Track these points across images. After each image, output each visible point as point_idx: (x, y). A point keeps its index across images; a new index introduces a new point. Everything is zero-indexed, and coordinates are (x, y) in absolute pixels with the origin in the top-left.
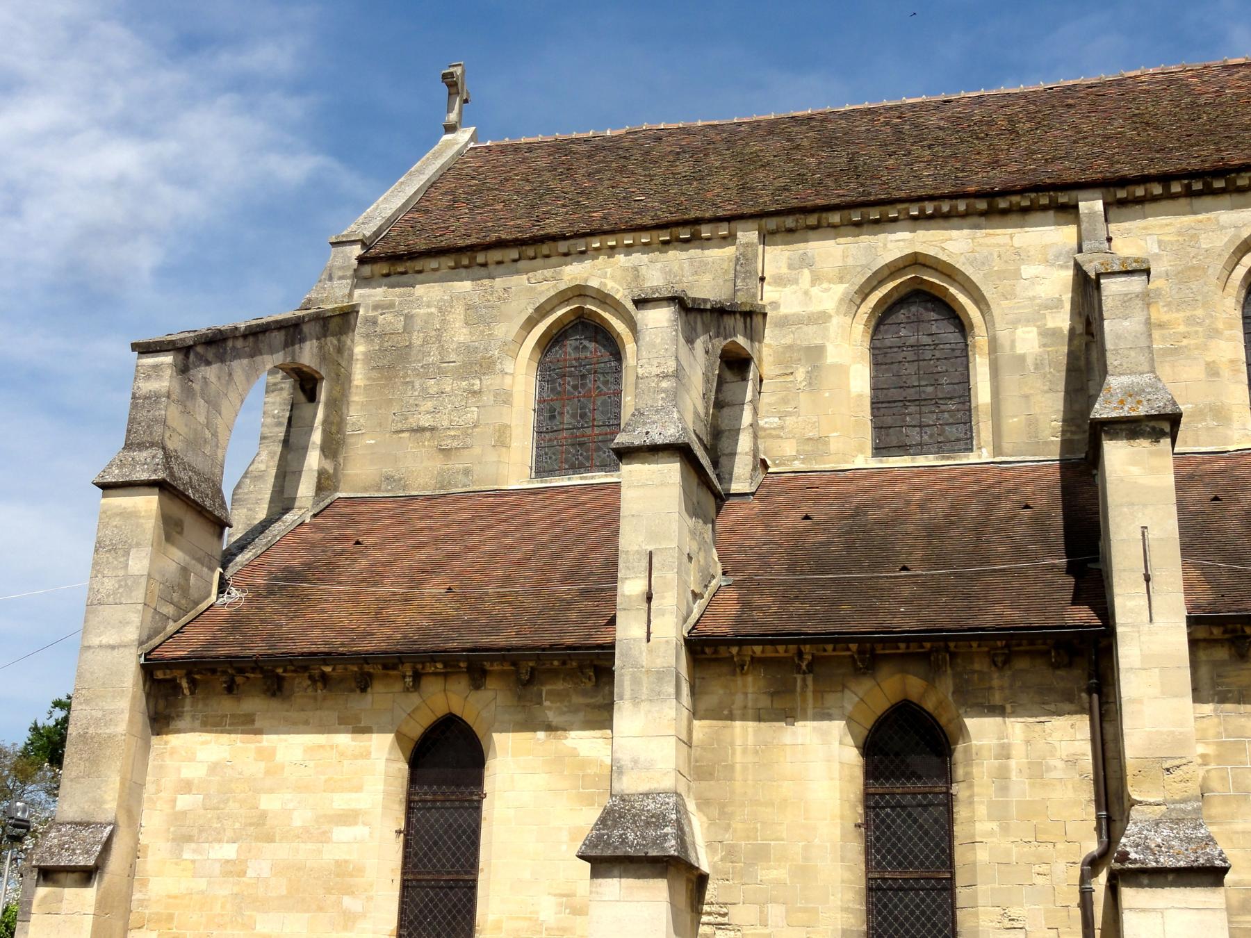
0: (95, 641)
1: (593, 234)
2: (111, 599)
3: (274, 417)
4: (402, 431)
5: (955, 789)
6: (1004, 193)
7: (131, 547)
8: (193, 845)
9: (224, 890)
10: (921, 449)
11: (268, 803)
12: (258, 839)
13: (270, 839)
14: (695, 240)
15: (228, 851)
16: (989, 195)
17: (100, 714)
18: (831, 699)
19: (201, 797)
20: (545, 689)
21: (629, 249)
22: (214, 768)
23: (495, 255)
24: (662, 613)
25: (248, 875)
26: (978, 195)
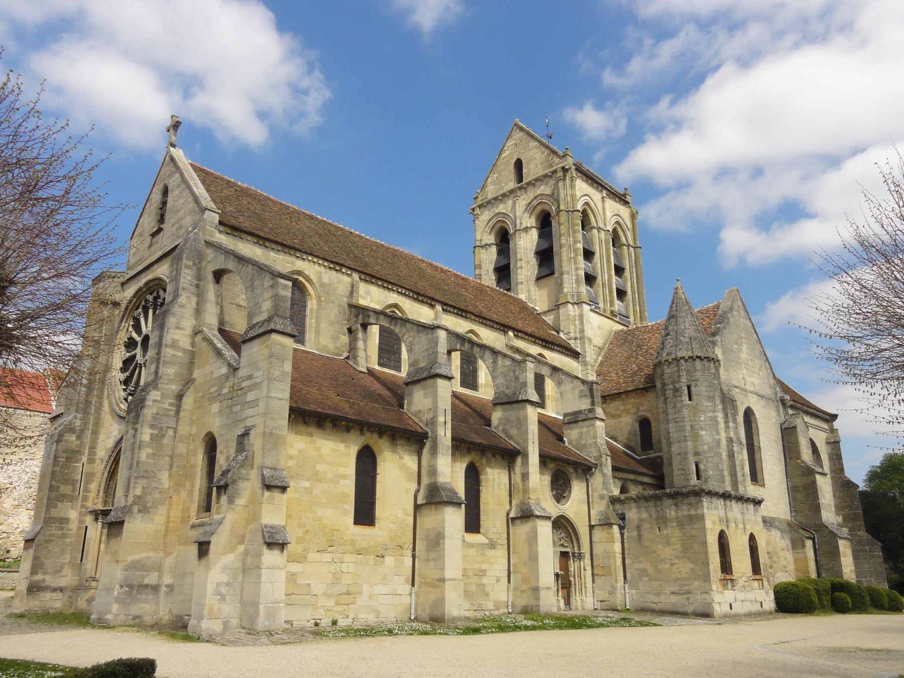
0: (273, 395)
1: (311, 254)
2: (278, 379)
3: (189, 280)
4: (233, 304)
5: (481, 488)
6: (422, 295)
7: (284, 359)
8: (294, 480)
10: (389, 368)
11: (319, 468)
13: (320, 481)
15: (307, 484)
16: (418, 294)
17: (277, 425)
18: (463, 459)
19: (296, 462)
20: (399, 442)
22: (300, 451)
23: (274, 246)
24: (448, 429)
25: (314, 493)
26: (416, 293)
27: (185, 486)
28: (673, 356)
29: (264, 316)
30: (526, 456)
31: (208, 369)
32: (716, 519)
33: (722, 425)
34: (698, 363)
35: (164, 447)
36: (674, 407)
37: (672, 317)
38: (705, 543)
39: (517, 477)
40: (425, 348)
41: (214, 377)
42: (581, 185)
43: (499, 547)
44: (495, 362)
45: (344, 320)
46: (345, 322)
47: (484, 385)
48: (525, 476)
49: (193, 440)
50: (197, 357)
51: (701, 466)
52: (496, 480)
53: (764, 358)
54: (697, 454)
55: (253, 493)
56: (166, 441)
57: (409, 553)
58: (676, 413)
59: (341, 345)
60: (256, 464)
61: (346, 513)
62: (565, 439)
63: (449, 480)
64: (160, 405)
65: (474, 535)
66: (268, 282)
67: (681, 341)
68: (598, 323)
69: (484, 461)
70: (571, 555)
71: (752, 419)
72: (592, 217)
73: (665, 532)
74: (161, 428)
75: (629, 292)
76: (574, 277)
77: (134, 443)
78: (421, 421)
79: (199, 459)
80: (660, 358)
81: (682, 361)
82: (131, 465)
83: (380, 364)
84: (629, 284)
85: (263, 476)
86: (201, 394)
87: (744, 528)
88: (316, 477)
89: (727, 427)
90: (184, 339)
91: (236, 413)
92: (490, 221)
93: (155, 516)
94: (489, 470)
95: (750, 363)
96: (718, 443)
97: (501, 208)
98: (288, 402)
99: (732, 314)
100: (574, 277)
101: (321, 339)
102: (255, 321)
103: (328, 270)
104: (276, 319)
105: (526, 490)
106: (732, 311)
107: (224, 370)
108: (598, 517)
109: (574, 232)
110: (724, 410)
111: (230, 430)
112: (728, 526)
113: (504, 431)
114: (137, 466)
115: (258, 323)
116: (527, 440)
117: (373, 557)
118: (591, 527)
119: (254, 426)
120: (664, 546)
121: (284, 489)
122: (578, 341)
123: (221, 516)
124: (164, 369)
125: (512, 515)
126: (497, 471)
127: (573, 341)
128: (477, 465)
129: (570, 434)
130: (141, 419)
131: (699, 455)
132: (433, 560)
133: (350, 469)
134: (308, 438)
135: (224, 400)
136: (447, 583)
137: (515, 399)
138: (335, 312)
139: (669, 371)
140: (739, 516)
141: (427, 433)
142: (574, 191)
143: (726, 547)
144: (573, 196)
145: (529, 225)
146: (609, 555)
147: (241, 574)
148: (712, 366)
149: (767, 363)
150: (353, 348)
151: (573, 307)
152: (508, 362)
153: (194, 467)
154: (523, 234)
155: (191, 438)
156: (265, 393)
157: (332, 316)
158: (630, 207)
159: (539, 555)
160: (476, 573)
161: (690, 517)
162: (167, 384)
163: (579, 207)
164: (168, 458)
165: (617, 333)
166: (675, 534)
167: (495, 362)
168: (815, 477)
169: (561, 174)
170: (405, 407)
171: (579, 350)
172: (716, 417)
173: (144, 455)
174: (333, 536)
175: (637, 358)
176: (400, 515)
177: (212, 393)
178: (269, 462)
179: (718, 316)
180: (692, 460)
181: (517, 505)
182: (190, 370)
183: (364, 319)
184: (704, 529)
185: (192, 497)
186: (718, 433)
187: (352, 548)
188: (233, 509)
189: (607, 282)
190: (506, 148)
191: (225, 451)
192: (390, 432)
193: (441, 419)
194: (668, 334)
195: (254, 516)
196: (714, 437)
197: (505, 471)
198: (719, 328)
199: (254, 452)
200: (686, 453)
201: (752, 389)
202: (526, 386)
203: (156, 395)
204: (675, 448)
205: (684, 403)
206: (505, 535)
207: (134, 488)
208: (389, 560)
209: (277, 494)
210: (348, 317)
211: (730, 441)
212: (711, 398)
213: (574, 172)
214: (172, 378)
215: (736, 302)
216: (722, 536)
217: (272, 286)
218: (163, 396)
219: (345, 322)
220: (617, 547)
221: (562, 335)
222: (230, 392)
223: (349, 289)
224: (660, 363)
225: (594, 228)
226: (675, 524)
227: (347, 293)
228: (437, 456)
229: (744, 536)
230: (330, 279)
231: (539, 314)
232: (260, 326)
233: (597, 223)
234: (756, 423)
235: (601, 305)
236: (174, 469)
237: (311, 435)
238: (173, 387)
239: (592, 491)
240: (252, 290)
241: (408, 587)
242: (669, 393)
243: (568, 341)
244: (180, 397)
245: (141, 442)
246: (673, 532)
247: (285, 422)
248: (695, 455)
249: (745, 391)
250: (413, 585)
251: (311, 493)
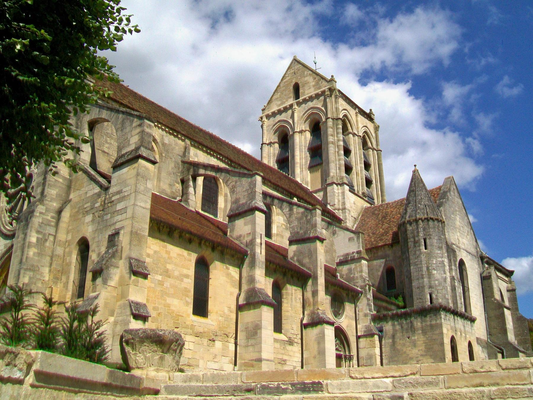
0: (139, 204)
2: (143, 193)
5: (283, 300)
9: (159, 289)
10: (209, 213)
11: (169, 267)
12: (166, 276)
14: (176, 136)
15: (159, 278)
16: (232, 161)
17: (141, 227)
21: (163, 130)
22: (155, 252)
25: (165, 285)
27: (61, 280)
28: (414, 218)
29: (133, 147)
30: (316, 278)
31: (83, 190)
32: (449, 327)
33: (447, 268)
34: (431, 223)
35: (47, 249)
36: (415, 254)
37: (413, 191)
38: (442, 344)
39: (309, 294)
40: (245, 189)
41: (88, 196)
42: (342, 102)
43: (295, 344)
44: (291, 210)
45: (178, 173)
46: (179, 174)
47: (276, 235)
48: (315, 293)
49: (69, 245)
50: (73, 184)
51: (434, 296)
52: (294, 295)
53: (470, 227)
54: (430, 287)
55: (122, 277)
56: (47, 244)
57: (233, 341)
58: (416, 258)
59: (176, 190)
60: (124, 255)
61: (187, 303)
62: (338, 274)
63: (263, 287)
64: (45, 217)
65: (278, 334)
66: (136, 122)
67: (419, 207)
68: (354, 200)
69: (285, 279)
70: (343, 357)
71: (463, 267)
72: (349, 125)
73: (413, 338)
74: (44, 235)
75: (374, 182)
76: (337, 165)
77: (24, 244)
78: (241, 243)
79: (74, 258)
80: (403, 220)
81: (420, 221)
82: (21, 260)
83: (202, 210)
84: (374, 175)
85: (131, 264)
86: (76, 210)
87: (466, 337)
88: (167, 274)
89: (451, 269)
90: (64, 170)
91: (106, 220)
92: (274, 125)
93: (38, 301)
94: (288, 286)
95: (461, 228)
96: (445, 279)
97: (283, 117)
98: (149, 211)
99: (450, 193)
100: (337, 165)
101: (162, 184)
102: (124, 152)
103: (168, 134)
104: (142, 148)
105: (315, 303)
106: (450, 191)
107: (97, 189)
108: (363, 330)
109: (338, 133)
110: (448, 256)
111: (101, 233)
112: (456, 334)
113: (298, 261)
114: (26, 260)
115: (126, 153)
116: (317, 266)
117: (206, 340)
118: (358, 337)
119: (122, 228)
120: (412, 348)
121: (145, 276)
122: (341, 211)
123: (97, 293)
124: (49, 190)
125: (305, 322)
126: (294, 288)
127: (337, 211)
128: (280, 282)
129: (341, 270)
130: (30, 225)
131: (432, 288)
132: (252, 345)
133: (191, 271)
134: (162, 243)
135: (96, 212)
136: (263, 362)
137: (307, 236)
138: (172, 165)
139: (411, 228)
140: (462, 328)
141: (247, 251)
142: (337, 105)
143: (455, 349)
144: (337, 109)
145: (304, 129)
146: (371, 357)
147: (111, 339)
148: (440, 225)
149: (472, 231)
150: (185, 193)
151: (337, 186)
152: (301, 210)
153: (69, 264)
155: (67, 244)
156: (132, 202)
157: (170, 168)
158: (373, 122)
159: (326, 350)
160: (280, 361)
161: (432, 326)
162: (50, 201)
163: (341, 116)
164: (48, 258)
165: (367, 209)
166: (420, 339)
167: (291, 210)
168: (503, 310)
169: (328, 93)
170: (228, 234)
171: (341, 217)
172: (443, 261)
173: (31, 252)
174: (178, 320)
175: (383, 225)
176: (226, 310)
177: (86, 208)
178: (134, 255)
179: (440, 195)
180: (427, 291)
181: (308, 315)
182: (68, 193)
183: (194, 171)
184: (442, 333)
185: (67, 287)
186: (445, 273)
187: (191, 331)
188: (106, 288)
189: (359, 172)
190: (287, 75)
191: (96, 249)
192: (220, 248)
193: (258, 241)
194: (409, 203)
195: (123, 295)
196: (442, 275)
197: (299, 288)
198: (442, 202)
199: (122, 247)
200: (423, 287)
201: (463, 247)
202: (316, 226)
203: (42, 209)
204: (415, 284)
206: (299, 336)
207: (24, 277)
208: (218, 344)
209: (141, 280)
210: (181, 171)
211: (453, 278)
212: (440, 248)
213: (338, 93)
214: (54, 197)
215: (452, 186)
216: (453, 339)
217: (140, 125)
218: (47, 210)
219: (179, 174)
220: (377, 351)
221: (329, 207)
222: (101, 205)
223: (183, 150)
224: (404, 223)
225: (350, 133)
226: (421, 331)
227: (181, 154)
228: (255, 268)
229: (465, 342)
230: (169, 141)
231: (311, 192)
232: (129, 155)
234: (466, 271)
235: (356, 188)
236: (54, 266)
237: (163, 241)
238: (55, 204)
239: (358, 311)
240: (122, 130)
241: (232, 366)
242: (411, 244)
243: (334, 211)
244: (59, 212)
245: (30, 242)
246: (419, 338)
247: (147, 226)
249: (459, 247)
250: (235, 364)
251: (163, 285)
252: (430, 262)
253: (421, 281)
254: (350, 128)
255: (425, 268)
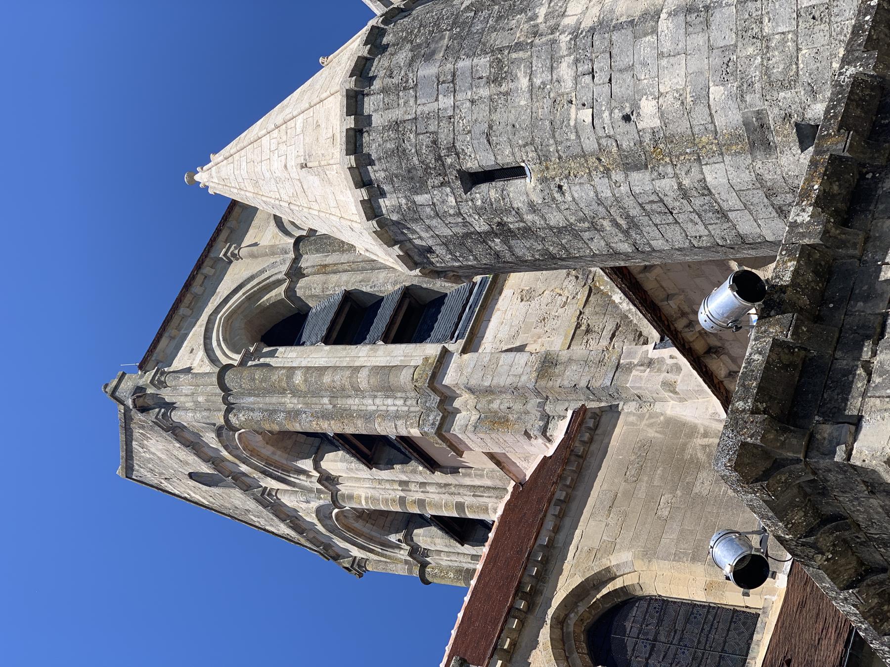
58: (595, 227)
131: (763, 126)
154: (343, 489)
205: (537, 199)
233: (279, 283)
248: (768, 147)
252: (590, 144)
253: (732, 201)
254: (273, 293)
255: (635, 176)
